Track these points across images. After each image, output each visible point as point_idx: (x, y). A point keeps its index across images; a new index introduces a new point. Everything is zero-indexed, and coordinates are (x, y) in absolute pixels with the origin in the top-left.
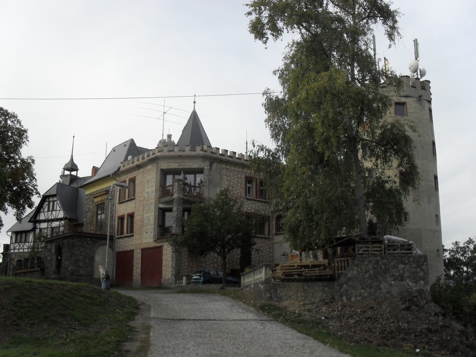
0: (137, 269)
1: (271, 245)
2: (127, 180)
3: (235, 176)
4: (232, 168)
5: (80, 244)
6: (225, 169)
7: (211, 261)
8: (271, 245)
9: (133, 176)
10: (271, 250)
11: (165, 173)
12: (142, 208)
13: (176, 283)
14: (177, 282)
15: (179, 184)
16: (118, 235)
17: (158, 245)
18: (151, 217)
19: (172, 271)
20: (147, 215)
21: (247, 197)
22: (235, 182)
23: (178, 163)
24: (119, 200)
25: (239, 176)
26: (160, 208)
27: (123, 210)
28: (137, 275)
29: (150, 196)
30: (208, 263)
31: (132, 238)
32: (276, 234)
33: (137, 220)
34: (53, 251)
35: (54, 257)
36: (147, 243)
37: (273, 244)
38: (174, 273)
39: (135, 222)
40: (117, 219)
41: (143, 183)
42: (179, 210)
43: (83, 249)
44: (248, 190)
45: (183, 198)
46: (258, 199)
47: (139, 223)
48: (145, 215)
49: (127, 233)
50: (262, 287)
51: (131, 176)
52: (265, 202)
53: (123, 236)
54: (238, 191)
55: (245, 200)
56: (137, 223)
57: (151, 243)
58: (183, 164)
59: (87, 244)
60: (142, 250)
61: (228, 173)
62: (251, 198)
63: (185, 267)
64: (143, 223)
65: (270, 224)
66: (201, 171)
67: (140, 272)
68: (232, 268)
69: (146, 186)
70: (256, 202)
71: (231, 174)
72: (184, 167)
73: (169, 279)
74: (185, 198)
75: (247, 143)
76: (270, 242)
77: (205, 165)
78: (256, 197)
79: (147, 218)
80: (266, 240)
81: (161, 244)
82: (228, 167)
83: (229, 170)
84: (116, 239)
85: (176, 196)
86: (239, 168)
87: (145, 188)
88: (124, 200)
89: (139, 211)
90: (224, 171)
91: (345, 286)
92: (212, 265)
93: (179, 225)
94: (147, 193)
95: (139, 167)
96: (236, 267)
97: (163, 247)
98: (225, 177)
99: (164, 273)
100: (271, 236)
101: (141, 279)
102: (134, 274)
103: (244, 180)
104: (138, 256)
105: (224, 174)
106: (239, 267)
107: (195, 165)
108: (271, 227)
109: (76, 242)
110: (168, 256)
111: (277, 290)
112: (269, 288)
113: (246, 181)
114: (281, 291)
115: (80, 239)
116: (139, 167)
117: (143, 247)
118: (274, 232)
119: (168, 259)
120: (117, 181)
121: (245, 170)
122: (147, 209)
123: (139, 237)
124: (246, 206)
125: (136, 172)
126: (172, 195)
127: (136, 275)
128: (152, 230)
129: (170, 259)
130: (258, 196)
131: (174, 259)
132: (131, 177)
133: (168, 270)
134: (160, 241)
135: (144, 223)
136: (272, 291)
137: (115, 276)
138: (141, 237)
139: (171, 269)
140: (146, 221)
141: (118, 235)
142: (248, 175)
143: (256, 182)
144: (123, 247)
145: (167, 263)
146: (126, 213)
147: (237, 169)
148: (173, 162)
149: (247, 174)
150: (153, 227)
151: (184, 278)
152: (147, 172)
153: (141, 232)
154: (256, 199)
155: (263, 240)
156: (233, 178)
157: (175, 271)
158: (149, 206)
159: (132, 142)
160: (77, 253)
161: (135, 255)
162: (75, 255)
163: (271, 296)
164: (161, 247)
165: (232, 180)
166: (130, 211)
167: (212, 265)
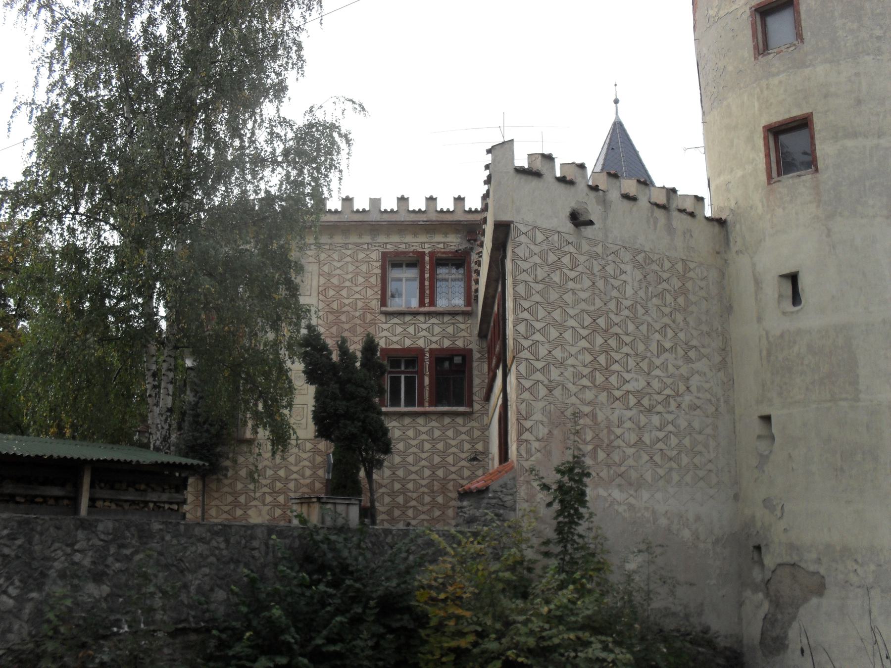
1: (477, 433)
4: (339, 239)
8: (477, 433)
25: (361, 256)
55: (383, 318)
70: (421, 318)
71: (336, 256)
76: (474, 424)
83: (327, 247)
86: (360, 236)
92: (269, 499)
103: (379, 264)
105: (311, 259)
121: (382, 239)
124: (385, 333)
130: (427, 300)
142: (390, 248)
155: (447, 420)
167: (269, 499)
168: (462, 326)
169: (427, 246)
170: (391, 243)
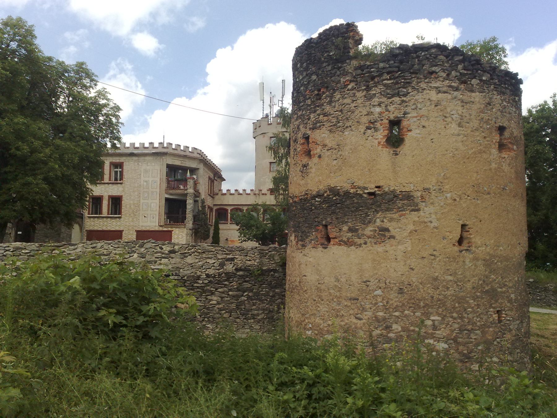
9: (118, 161)
12: (136, 193)
16: (89, 214)
18: (152, 205)
20: (146, 201)
29: (150, 185)
31: (118, 219)
36: (147, 226)
41: (138, 171)
47: (132, 207)
48: (142, 201)
56: (128, 206)
60: (138, 232)
69: (142, 174)
77: (201, 166)
81: (170, 229)
84: (87, 218)
88: (102, 182)
97: (173, 232)
107: (193, 165)
110: (181, 240)
122: (146, 196)
123: (131, 219)
125: (124, 158)
132: (114, 161)
138: (135, 219)
141: (89, 214)
152: (145, 163)
164: (171, 232)
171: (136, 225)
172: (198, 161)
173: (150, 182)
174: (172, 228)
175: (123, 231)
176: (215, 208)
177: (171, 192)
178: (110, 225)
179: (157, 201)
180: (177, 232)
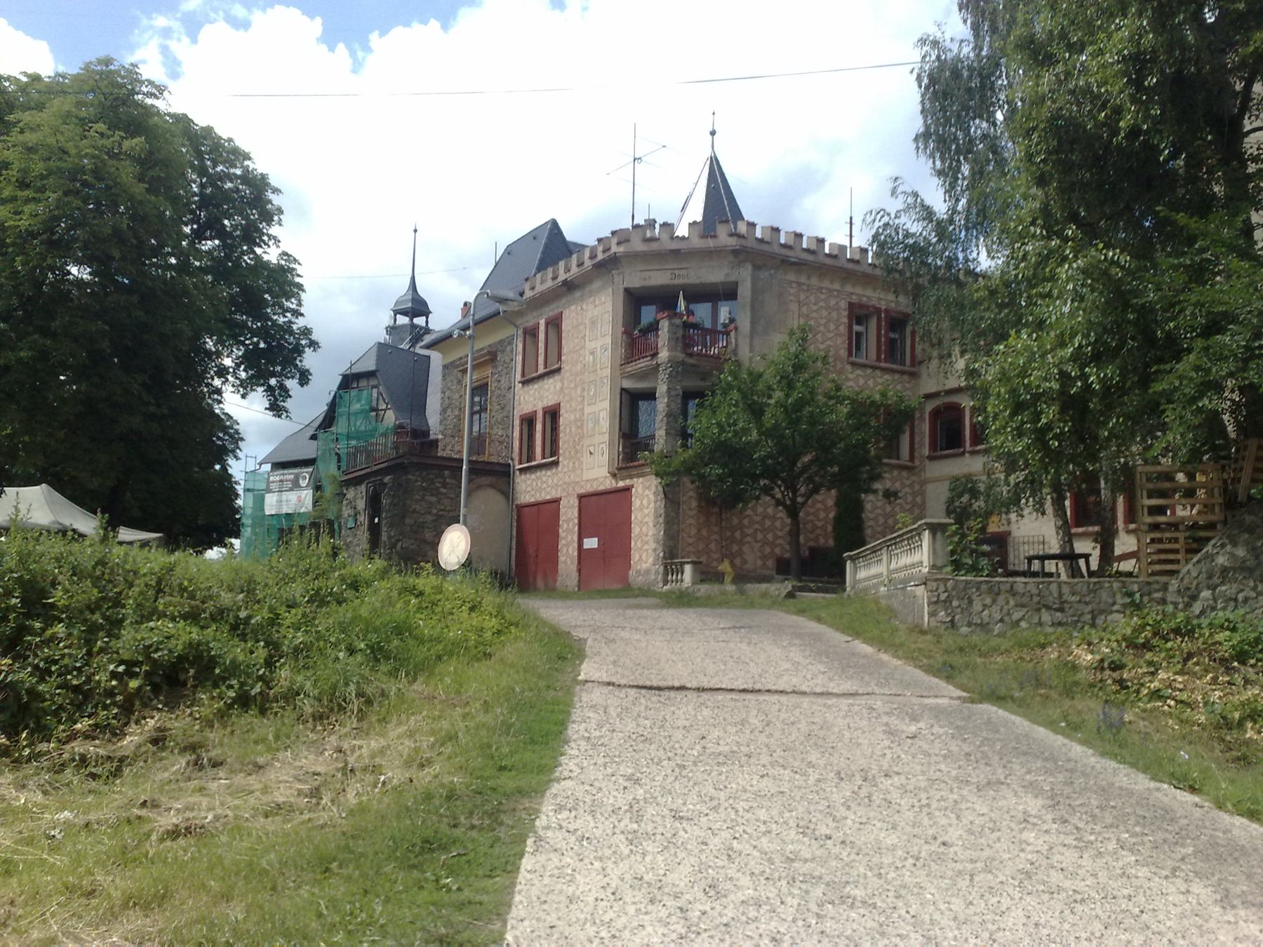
0: (567, 545)
1: (917, 487)
2: (542, 322)
3: (822, 304)
4: (814, 281)
5: (424, 484)
6: (794, 285)
7: (757, 526)
8: (917, 487)
10: (918, 499)
11: (635, 300)
13: (666, 582)
14: (670, 577)
15: (671, 325)
17: (621, 484)
19: (655, 550)
21: (853, 359)
22: (821, 318)
23: (670, 272)
24: (523, 375)
25: (833, 302)
26: (623, 390)
27: (532, 399)
28: (569, 562)
30: (749, 531)
32: (931, 458)
33: (567, 422)
34: (361, 504)
35: (363, 518)
37: (923, 483)
38: (661, 554)
39: (561, 428)
40: (517, 422)
41: (581, 327)
42: (673, 393)
43: (433, 499)
44: (855, 342)
45: (683, 363)
46: (883, 365)
47: (573, 429)
48: (588, 410)
49: (544, 458)
50: (920, 591)
51: (550, 311)
52: (902, 373)
53: (533, 463)
54: (829, 343)
55: (849, 367)
56: (568, 430)
57: (601, 480)
58: (684, 272)
59: (444, 485)
60: (581, 497)
61: (802, 297)
62: (862, 360)
63: (691, 541)
64: (582, 428)
65: (916, 430)
66: (729, 293)
67: (576, 553)
68: (812, 544)
70: (878, 373)
71: (812, 299)
72: (686, 281)
73: (648, 572)
74: (690, 361)
75: (851, 223)
76: (914, 478)
77: (744, 277)
78: (878, 359)
79: (590, 417)
80: (904, 473)
81: (628, 482)
82: (803, 279)
83: (805, 287)
85: (664, 355)
86: (832, 282)
87: (587, 339)
89: (571, 399)
90: (792, 291)
91: (1206, 594)
92: (760, 536)
93: (673, 432)
94: (592, 353)
95: (569, 287)
96: (822, 541)
97: (634, 490)
98: (794, 307)
99: (635, 556)
100: (917, 463)
101: (579, 571)
102: (562, 559)
103: (846, 313)
104: (569, 515)
105: (792, 298)
106: (831, 542)
107: (714, 274)
108: (917, 439)
109: (417, 481)
110: (646, 511)
111: (970, 601)
112: (943, 597)
113: (850, 317)
114: (985, 606)
115: (424, 473)
116: (569, 287)
117: (582, 491)
118: (926, 452)
119: (646, 519)
120: (516, 326)
121: (849, 288)
123: (571, 465)
126: (655, 355)
127: (565, 562)
128: (604, 446)
129: (650, 520)
131: (661, 520)
132: (551, 314)
133: (646, 547)
134: (625, 473)
135: (585, 431)
136: (955, 603)
137: (513, 563)
138: (577, 464)
139: (653, 545)
140: (591, 425)
142: (855, 299)
143: (879, 319)
144: (533, 493)
145: (644, 529)
146: (539, 407)
147: (826, 284)
148: (656, 267)
149: (854, 297)
150: (606, 438)
151: (688, 569)
153: (577, 452)
154: (876, 364)
155: (895, 473)
156: (815, 308)
157: (664, 550)
158: (596, 386)
159: (553, 228)
160: (418, 507)
161: (562, 510)
162: (414, 511)
163: (952, 621)
164: (628, 489)
165: (814, 315)
166: (550, 401)
167: (760, 536)
168: (908, 385)
169: (883, 303)
170: (857, 295)
171: (578, 480)
172: (731, 258)
173: (599, 353)
174: (631, 477)
175: (560, 499)
176: (930, 406)
177: (630, 368)
178: (545, 486)
179: (606, 404)
180: (640, 490)
